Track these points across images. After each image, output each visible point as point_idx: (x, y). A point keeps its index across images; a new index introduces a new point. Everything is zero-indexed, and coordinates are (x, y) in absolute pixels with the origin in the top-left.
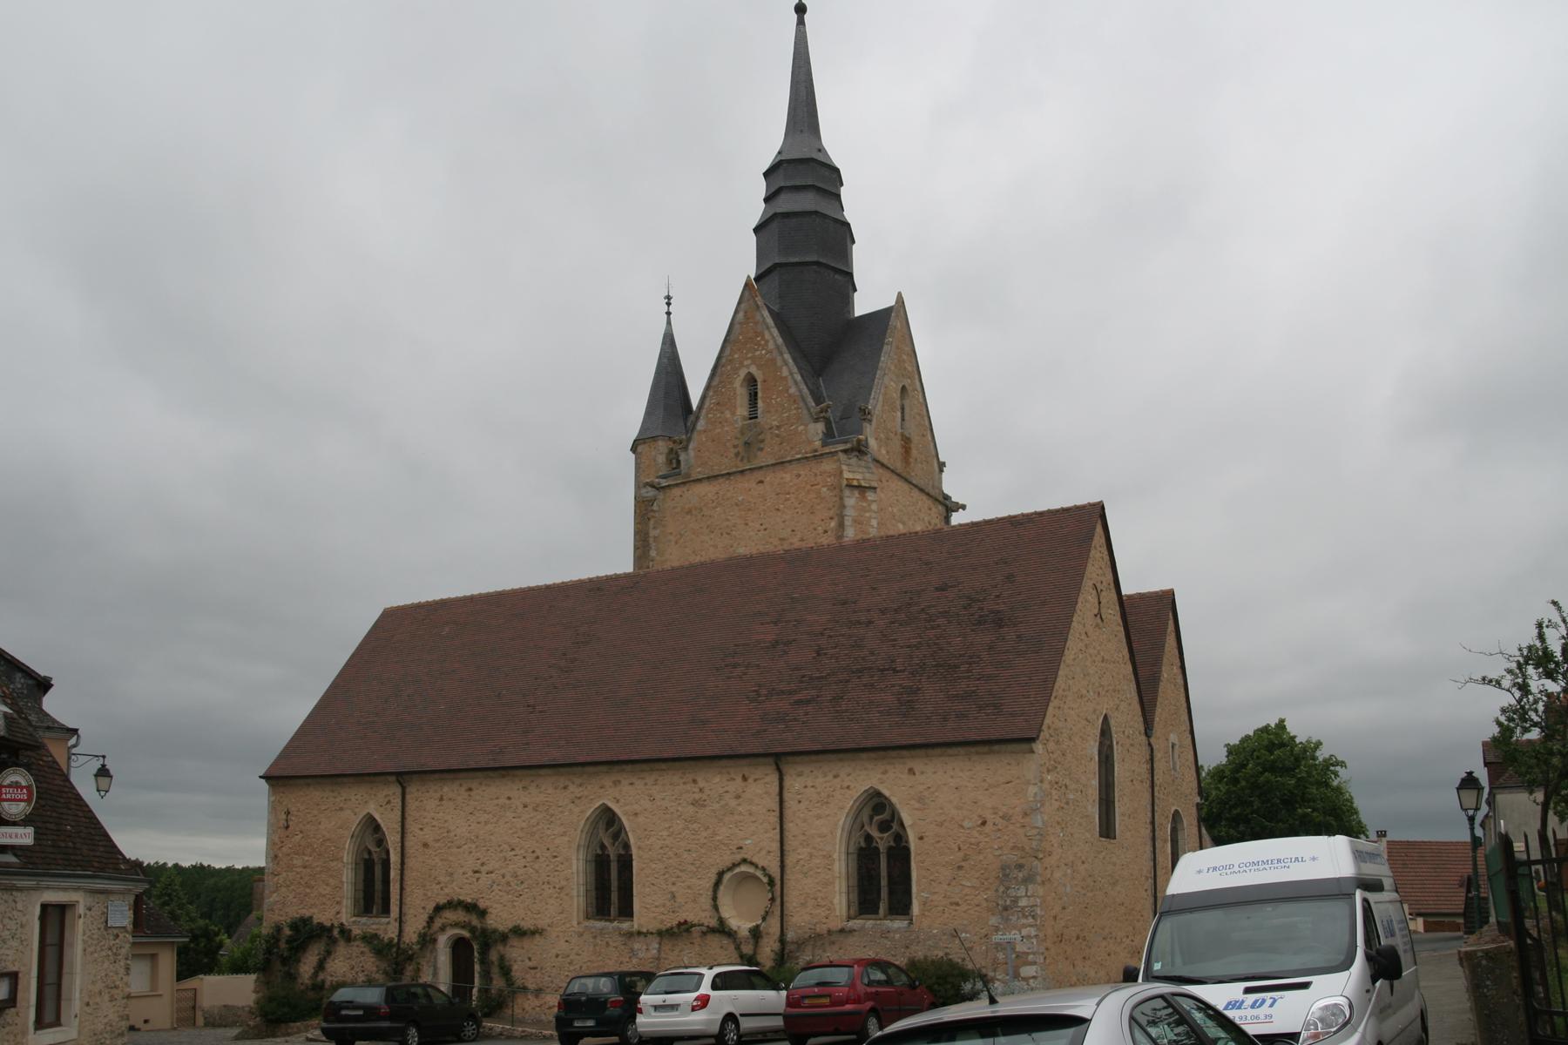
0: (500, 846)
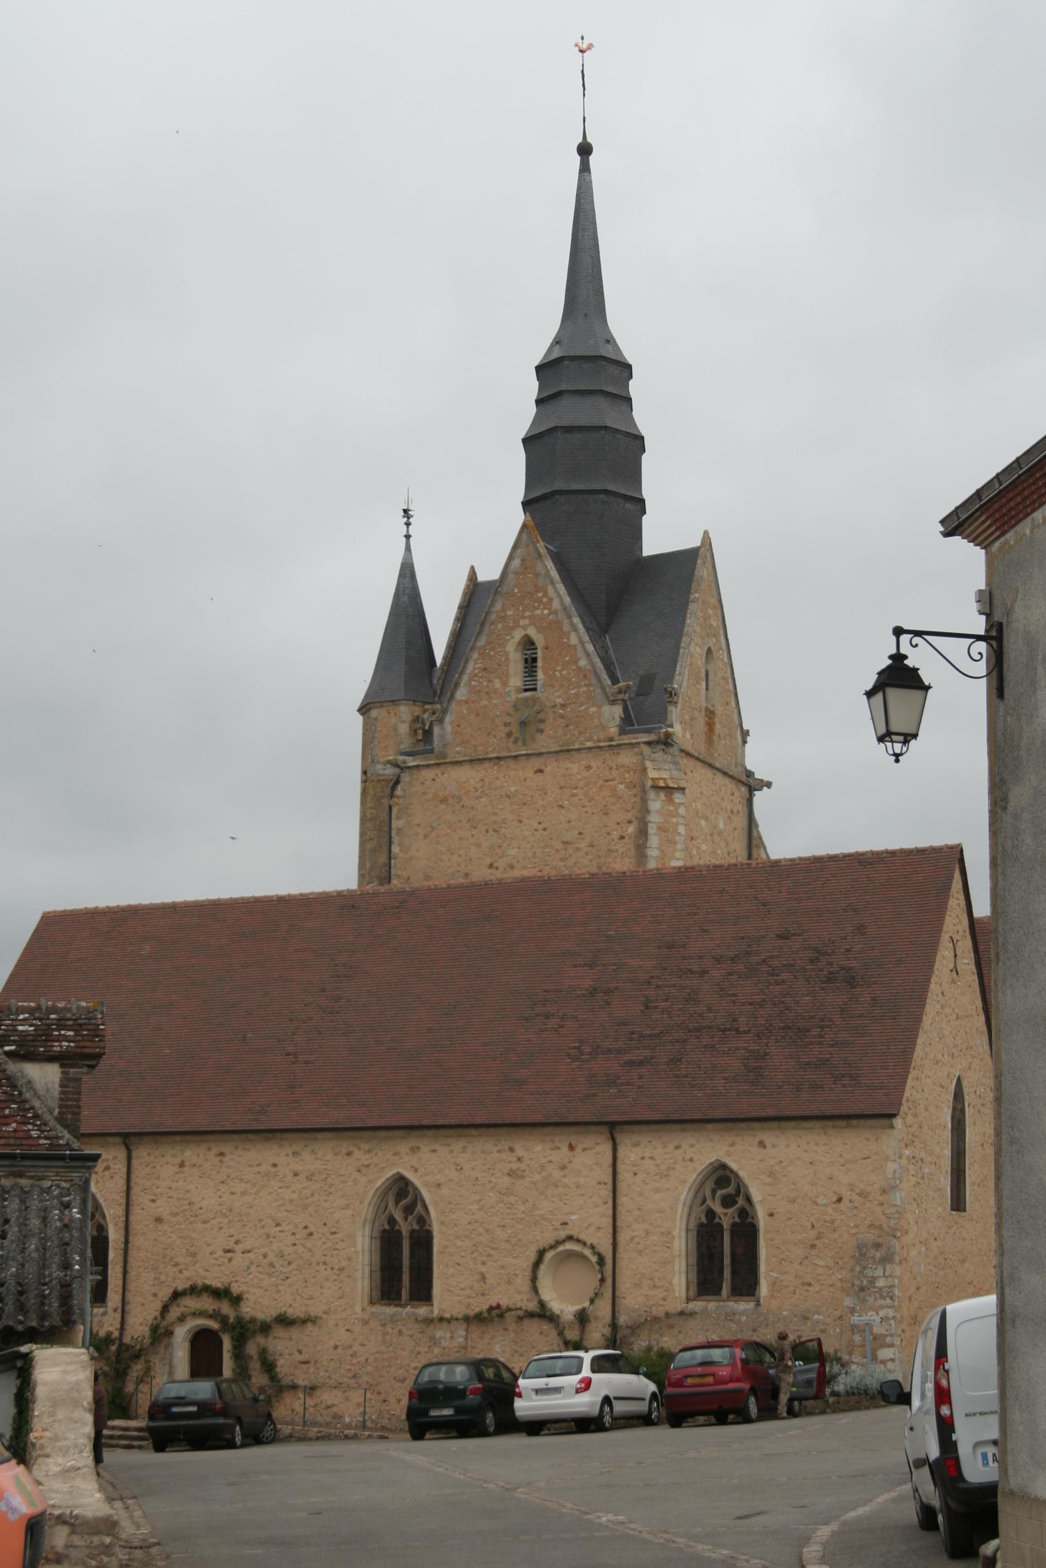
0: (261, 1221)
